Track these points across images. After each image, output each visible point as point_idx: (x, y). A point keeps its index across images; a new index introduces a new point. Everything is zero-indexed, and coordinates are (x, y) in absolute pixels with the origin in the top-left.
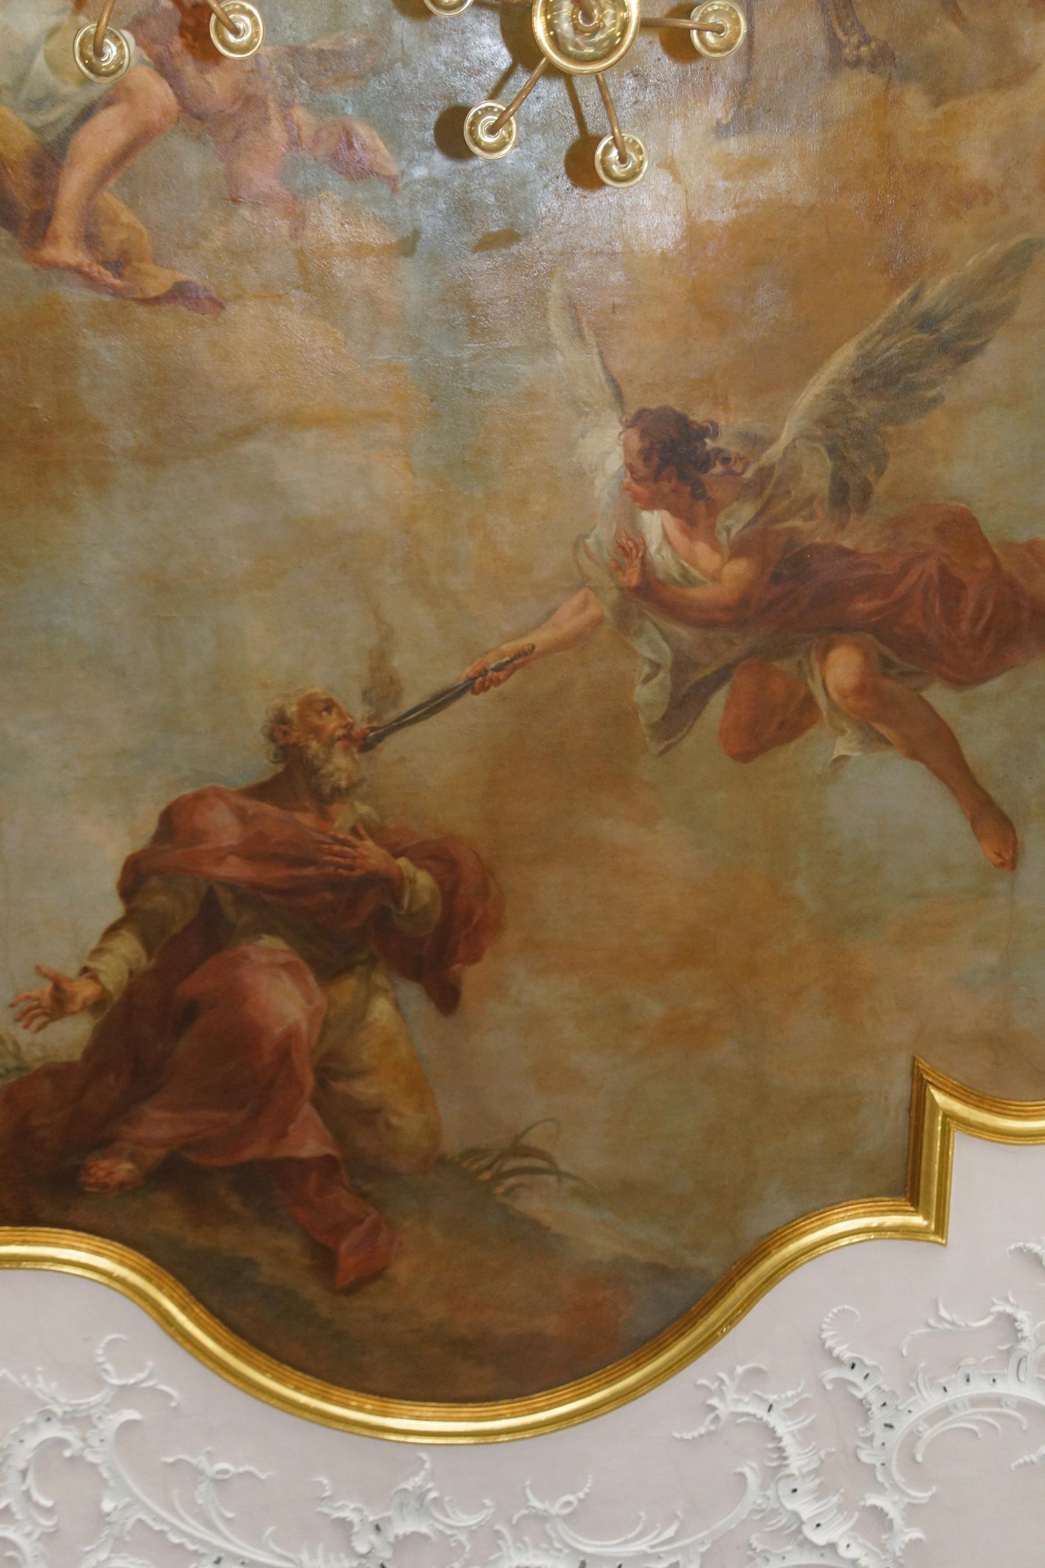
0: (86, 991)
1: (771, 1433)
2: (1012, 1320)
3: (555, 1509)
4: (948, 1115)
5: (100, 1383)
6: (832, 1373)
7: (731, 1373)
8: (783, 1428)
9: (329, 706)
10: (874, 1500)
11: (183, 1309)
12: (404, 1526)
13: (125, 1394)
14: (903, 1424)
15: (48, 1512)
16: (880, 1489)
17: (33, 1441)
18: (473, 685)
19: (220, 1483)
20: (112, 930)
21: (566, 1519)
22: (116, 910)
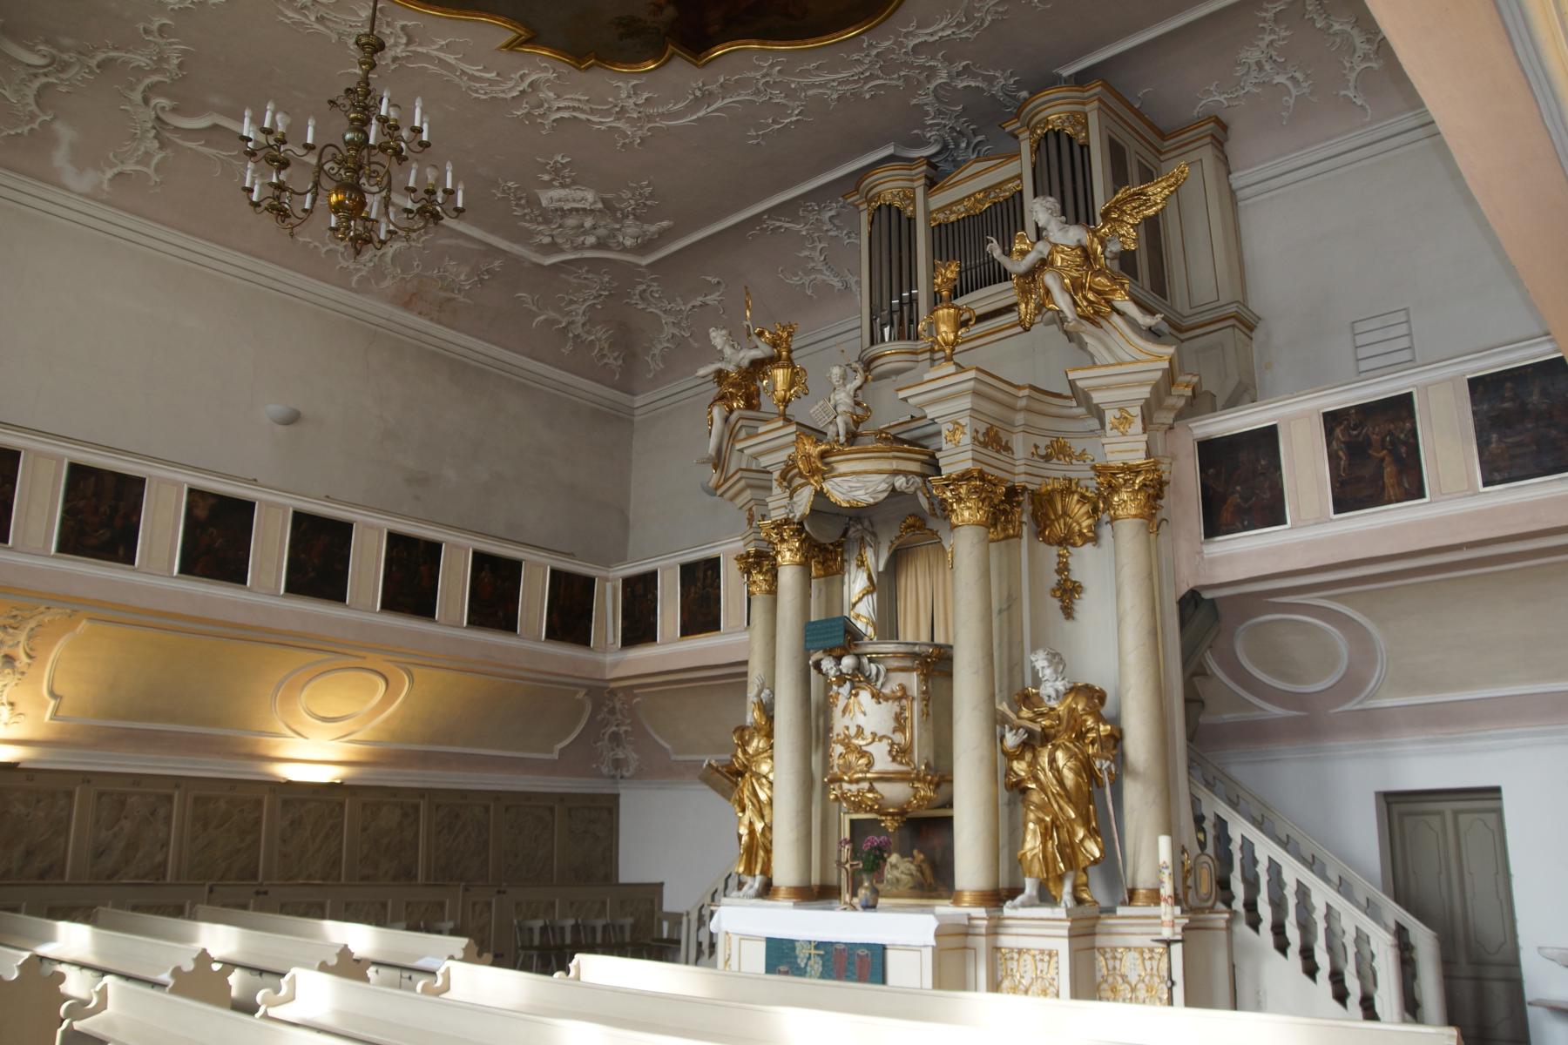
3: (911, 29)
12: (874, 52)
15: (781, 93)
19: (817, 68)
21: (917, 28)
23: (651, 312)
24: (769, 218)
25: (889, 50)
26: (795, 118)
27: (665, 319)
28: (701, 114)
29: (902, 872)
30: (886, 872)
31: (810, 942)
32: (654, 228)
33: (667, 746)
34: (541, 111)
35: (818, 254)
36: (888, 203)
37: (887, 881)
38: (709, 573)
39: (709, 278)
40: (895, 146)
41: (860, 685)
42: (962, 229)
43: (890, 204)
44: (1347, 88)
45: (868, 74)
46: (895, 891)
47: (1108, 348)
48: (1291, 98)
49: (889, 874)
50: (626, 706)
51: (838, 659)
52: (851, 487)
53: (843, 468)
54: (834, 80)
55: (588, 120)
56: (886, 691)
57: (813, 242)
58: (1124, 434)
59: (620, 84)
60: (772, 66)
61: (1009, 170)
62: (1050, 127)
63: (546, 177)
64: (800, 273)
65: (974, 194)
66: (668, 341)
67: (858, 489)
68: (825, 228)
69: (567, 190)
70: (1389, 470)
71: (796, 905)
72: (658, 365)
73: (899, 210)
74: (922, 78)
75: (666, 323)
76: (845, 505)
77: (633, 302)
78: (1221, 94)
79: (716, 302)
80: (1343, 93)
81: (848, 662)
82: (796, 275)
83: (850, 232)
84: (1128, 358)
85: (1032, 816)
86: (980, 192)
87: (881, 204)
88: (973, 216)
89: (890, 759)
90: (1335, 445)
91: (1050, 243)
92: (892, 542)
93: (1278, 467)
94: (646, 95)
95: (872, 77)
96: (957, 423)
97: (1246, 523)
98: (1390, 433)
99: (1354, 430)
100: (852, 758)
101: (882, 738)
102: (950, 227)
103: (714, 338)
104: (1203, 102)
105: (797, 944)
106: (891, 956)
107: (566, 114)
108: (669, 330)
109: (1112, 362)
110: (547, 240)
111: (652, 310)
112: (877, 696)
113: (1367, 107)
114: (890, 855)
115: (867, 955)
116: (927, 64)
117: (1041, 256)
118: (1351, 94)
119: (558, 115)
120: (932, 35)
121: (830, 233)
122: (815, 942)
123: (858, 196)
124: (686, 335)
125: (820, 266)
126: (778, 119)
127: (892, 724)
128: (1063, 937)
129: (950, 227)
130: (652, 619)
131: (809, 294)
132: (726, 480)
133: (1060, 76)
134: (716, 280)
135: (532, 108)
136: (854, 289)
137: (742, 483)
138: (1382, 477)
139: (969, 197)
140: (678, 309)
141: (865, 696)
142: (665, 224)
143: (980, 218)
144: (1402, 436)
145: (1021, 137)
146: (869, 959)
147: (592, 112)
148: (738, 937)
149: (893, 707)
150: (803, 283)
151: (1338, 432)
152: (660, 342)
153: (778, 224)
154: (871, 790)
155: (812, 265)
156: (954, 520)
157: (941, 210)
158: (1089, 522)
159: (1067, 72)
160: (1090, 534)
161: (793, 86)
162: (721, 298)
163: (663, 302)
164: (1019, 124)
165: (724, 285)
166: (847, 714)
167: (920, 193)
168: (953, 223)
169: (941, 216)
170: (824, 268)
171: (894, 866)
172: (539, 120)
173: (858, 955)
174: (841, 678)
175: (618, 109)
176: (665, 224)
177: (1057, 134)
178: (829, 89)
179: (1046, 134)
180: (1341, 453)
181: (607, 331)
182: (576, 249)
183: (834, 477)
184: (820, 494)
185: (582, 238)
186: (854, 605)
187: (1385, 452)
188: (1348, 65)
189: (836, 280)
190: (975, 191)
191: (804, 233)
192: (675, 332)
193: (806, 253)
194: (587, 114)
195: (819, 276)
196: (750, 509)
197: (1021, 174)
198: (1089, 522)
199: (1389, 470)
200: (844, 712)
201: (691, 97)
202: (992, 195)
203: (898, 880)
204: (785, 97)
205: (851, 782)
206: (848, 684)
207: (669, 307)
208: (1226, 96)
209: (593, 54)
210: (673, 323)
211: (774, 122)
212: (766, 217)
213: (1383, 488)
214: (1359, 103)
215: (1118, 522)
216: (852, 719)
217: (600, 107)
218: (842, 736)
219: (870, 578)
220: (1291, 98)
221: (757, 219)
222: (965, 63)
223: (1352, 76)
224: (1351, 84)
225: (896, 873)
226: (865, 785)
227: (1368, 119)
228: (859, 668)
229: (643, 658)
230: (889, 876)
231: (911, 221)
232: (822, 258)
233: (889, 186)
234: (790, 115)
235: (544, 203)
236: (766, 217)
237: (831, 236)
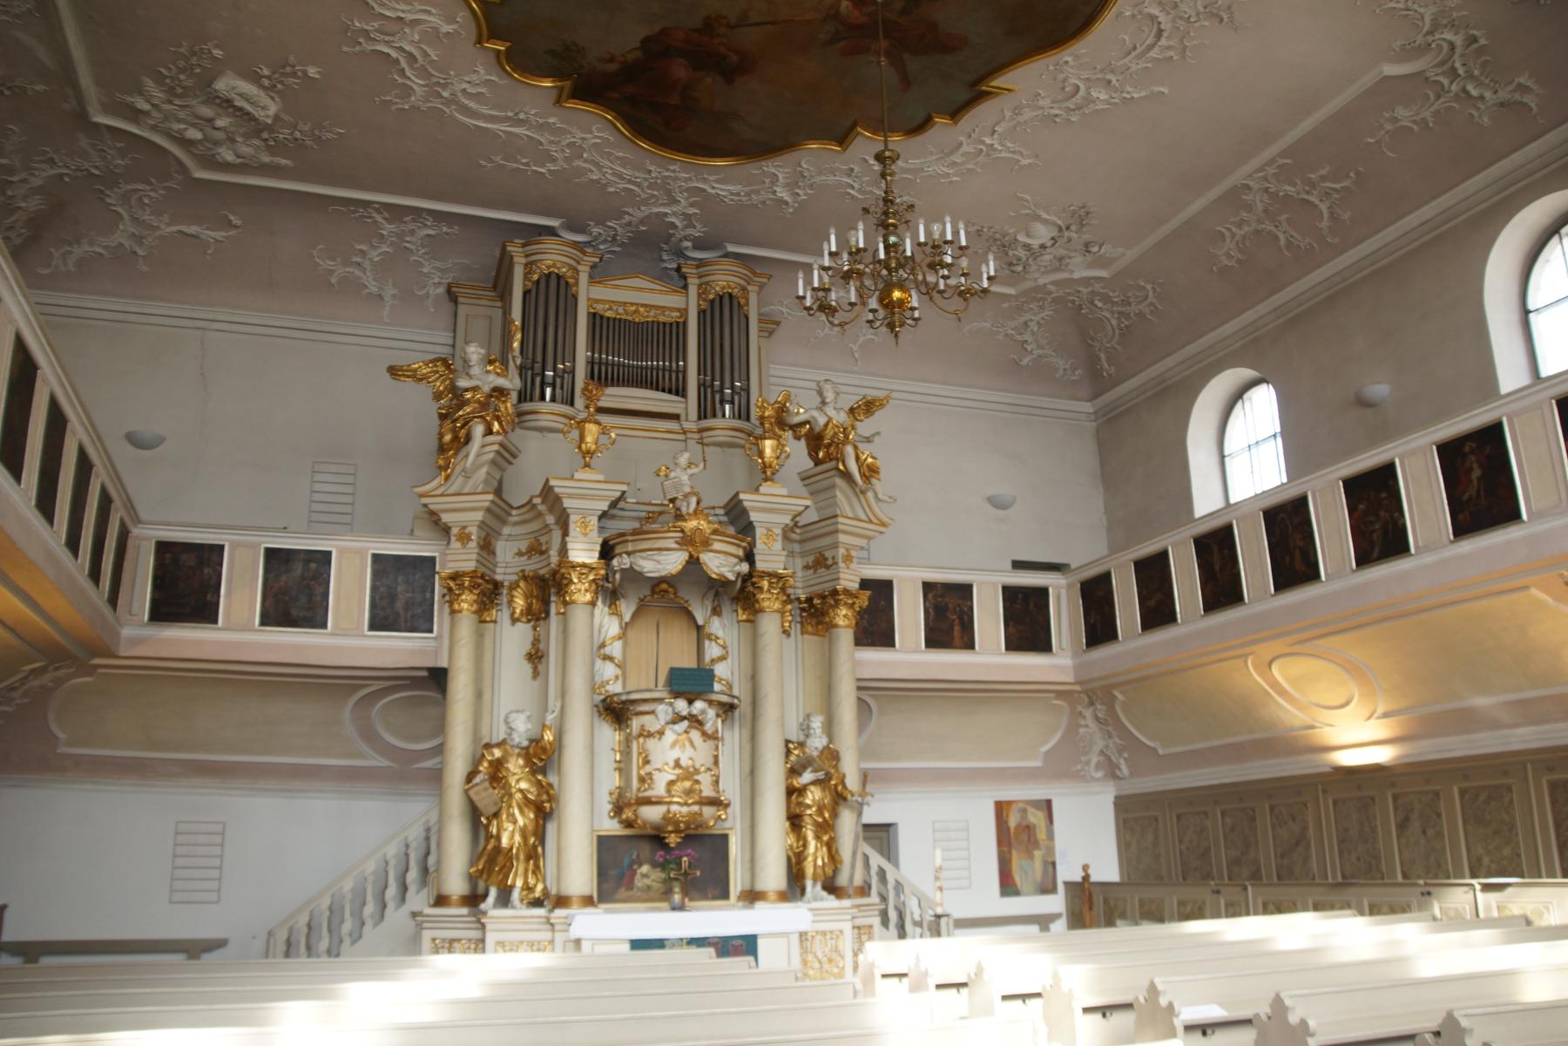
0: (622, 59)
1: (776, 175)
2: (852, 170)
4: (859, 133)
5: (591, 133)
6: (799, 169)
7: (772, 163)
8: (781, 176)
9: (725, 18)
10: (797, 191)
11: (623, 126)
13: (597, 137)
14: (813, 181)
16: (800, 189)
17: (568, 141)
18: (771, 23)
19: (618, 158)
20: (636, 49)
22: (638, 45)
23: (115, 211)
24: (379, 212)
25: (676, 179)
26: (543, 170)
27: (127, 225)
28: (490, 126)
29: (653, 881)
30: (636, 881)
31: (681, 939)
32: (266, 159)
33: (62, 736)
34: (380, 37)
35: (376, 253)
36: (561, 274)
37: (638, 889)
38: (313, 565)
39: (232, 218)
40: (563, 223)
41: (695, 724)
42: (627, 327)
43: (562, 276)
44: (855, 343)
45: (639, 180)
46: (646, 896)
47: (851, 505)
48: (823, 331)
49: (639, 882)
50: (50, 684)
51: (691, 702)
52: (721, 564)
53: (717, 546)
54: (612, 169)
55: (403, 70)
56: (710, 732)
57: (385, 243)
58: (848, 568)
59: (482, 72)
60: (597, 137)
61: (673, 300)
62: (730, 291)
63: (266, 72)
64: (339, 260)
65: (637, 304)
66: (105, 247)
67: (725, 566)
68: (407, 239)
69: (261, 91)
70: (957, 628)
71: (745, 907)
72: (65, 265)
73: (567, 283)
74: (660, 202)
75: (122, 231)
76: (714, 576)
77: (108, 192)
78: (787, 307)
79: (212, 241)
80: (851, 345)
81: (699, 705)
82: (332, 259)
83: (425, 253)
84: (863, 517)
85: (810, 835)
86: (642, 305)
87: (553, 272)
88: (630, 322)
89: (712, 788)
90: (927, 604)
91: (827, 415)
92: (642, 600)
93: (892, 609)
94: (484, 90)
95: (639, 185)
96: (772, 531)
97: (870, 641)
98: (959, 605)
99: (940, 596)
100: (687, 784)
101: (709, 769)
102: (605, 321)
103: (473, 353)
104: (773, 307)
105: (666, 942)
106: (761, 943)
107: (394, 54)
108: (120, 238)
109: (850, 515)
110: (146, 107)
111: (120, 210)
112: (704, 734)
113: (859, 362)
114: (640, 865)
115: (742, 945)
116: (678, 199)
117: (812, 420)
118: (855, 349)
119: (386, 50)
120: (713, 188)
121: (407, 245)
122: (687, 939)
123: (521, 250)
124: (141, 252)
125: (367, 264)
126: (532, 163)
127: (711, 760)
128: (876, 916)
129: (605, 321)
130: (209, 597)
131: (332, 282)
132: (442, 495)
133: (726, 247)
134: (239, 222)
135: (376, 30)
136: (386, 299)
137: (487, 504)
138: (952, 631)
139: (632, 304)
140: (155, 224)
141: (695, 735)
142: (284, 162)
143: (636, 326)
144: (965, 609)
145: (690, 280)
146: (744, 947)
147: (423, 72)
148: (591, 942)
149: (711, 743)
150: (334, 271)
151: (930, 596)
152: (91, 243)
153: (375, 215)
154: (701, 809)
155: (359, 260)
156: (757, 606)
157: (598, 301)
158: (790, 618)
159: (732, 248)
160: (788, 628)
161: (585, 155)
162: (222, 239)
163: (144, 210)
164: (695, 271)
165: (240, 230)
166: (677, 748)
167: (583, 278)
168: (608, 318)
169: (600, 308)
170: (368, 268)
171: (645, 876)
172: (361, 40)
173: (733, 945)
174: (678, 718)
175: (442, 81)
176: (284, 162)
177: (730, 295)
178: (600, 171)
179: (724, 293)
180: (931, 610)
181: (40, 204)
182: (154, 128)
183: (711, 551)
184: (693, 562)
185: (182, 126)
186: (603, 645)
187: (955, 617)
188: (864, 331)
189: (373, 283)
190: (627, 301)
191: (384, 233)
192: (123, 241)
193: (364, 247)
194: (412, 68)
195: (358, 272)
196: (465, 527)
197: (686, 310)
198: (790, 618)
199: (957, 628)
200: (674, 745)
201: (510, 114)
202: (652, 313)
203: (649, 887)
204: (565, 157)
205: (686, 804)
206: (685, 724)
207: (146, 217)
208: (788, 310)
209: (508, 44)
210: (133, 234)
211: (523, 164)
212: (376, 206)
213: (953, 638)
214: (856, 356)
215: (835, 630)
216: (683, 752)
217: (430, 70)
218: (672, 764)
219: (621, 627)
220: (823, 331)
221: (366, 204)
222: (697, 211)
223: (861, 340)
224: (858, 344)
225: (647, 881)
226: (696, 808)
227: (856, 368)
228: (703, 712)
229: (184, 638)
230: (640, 884)
231: (575, 297)
232: (376, 260)
233: (553, 256)
234: (543, 166)
235: (221, 85)
236: (376, 206)
237: (405, 247)
